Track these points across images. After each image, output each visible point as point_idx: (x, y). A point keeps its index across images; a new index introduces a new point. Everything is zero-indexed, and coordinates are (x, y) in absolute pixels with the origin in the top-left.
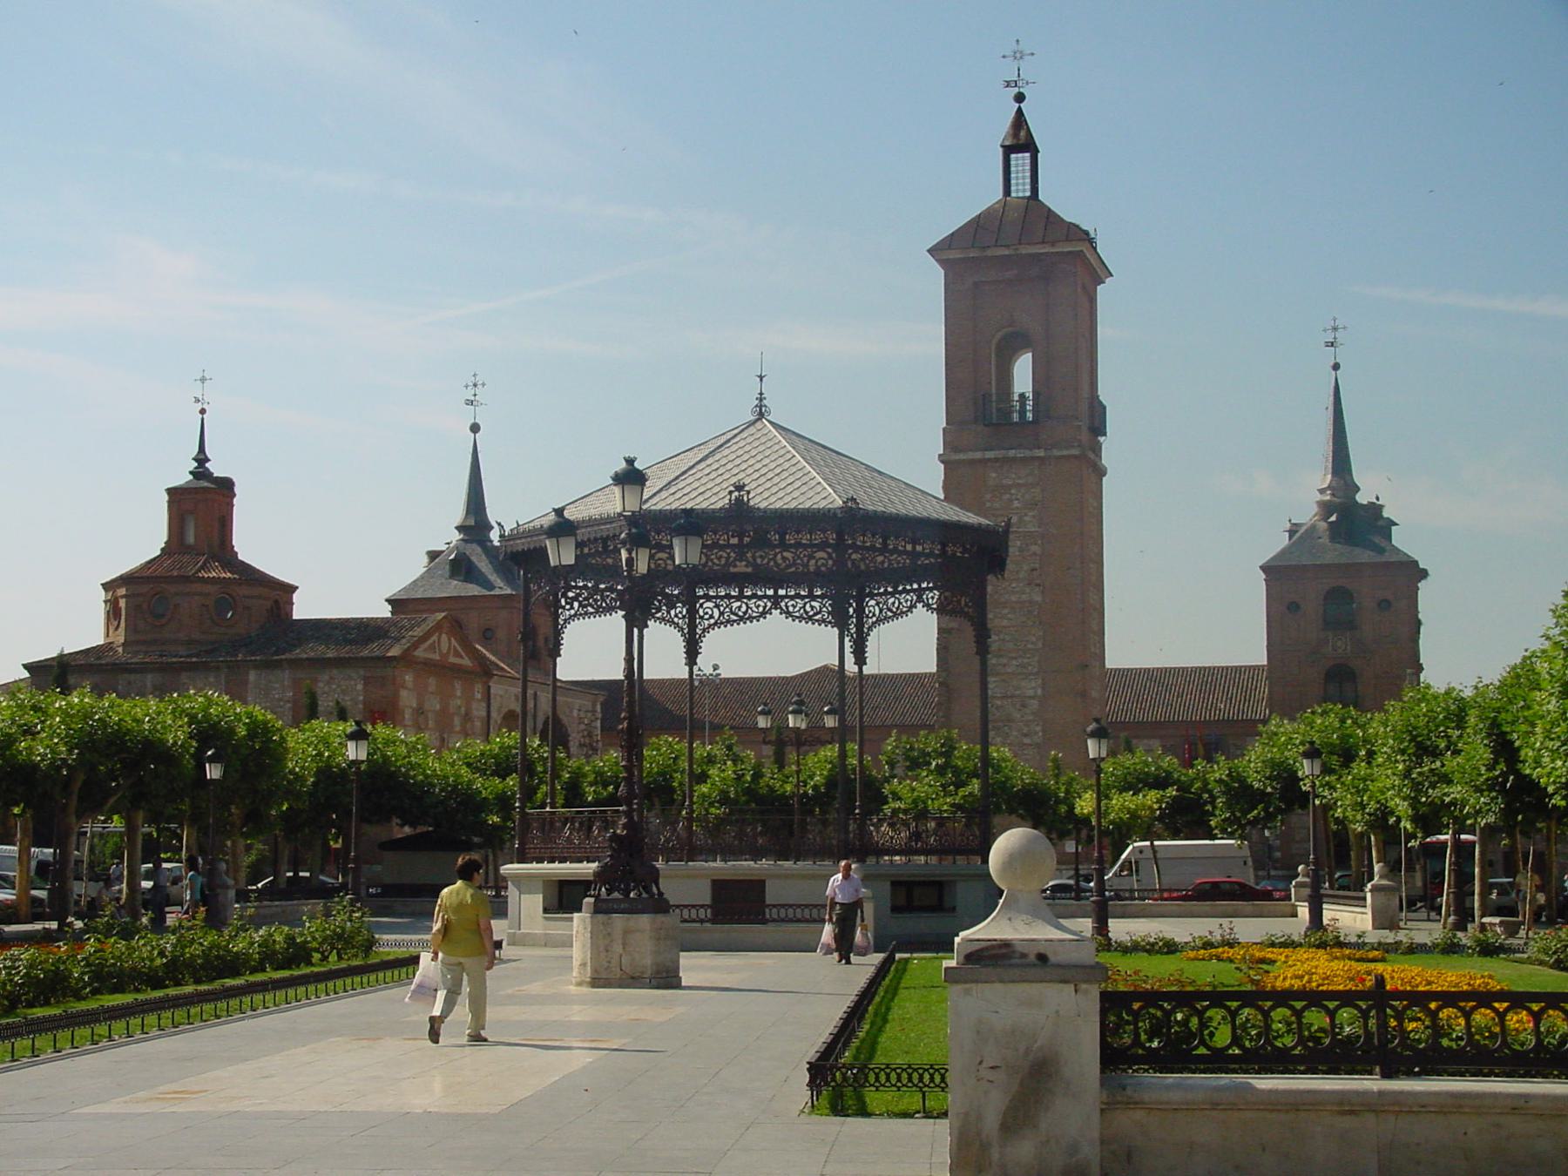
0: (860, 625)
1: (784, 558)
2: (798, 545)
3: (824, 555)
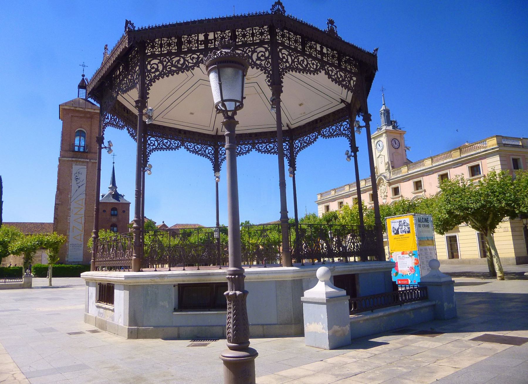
0: (292, 153)
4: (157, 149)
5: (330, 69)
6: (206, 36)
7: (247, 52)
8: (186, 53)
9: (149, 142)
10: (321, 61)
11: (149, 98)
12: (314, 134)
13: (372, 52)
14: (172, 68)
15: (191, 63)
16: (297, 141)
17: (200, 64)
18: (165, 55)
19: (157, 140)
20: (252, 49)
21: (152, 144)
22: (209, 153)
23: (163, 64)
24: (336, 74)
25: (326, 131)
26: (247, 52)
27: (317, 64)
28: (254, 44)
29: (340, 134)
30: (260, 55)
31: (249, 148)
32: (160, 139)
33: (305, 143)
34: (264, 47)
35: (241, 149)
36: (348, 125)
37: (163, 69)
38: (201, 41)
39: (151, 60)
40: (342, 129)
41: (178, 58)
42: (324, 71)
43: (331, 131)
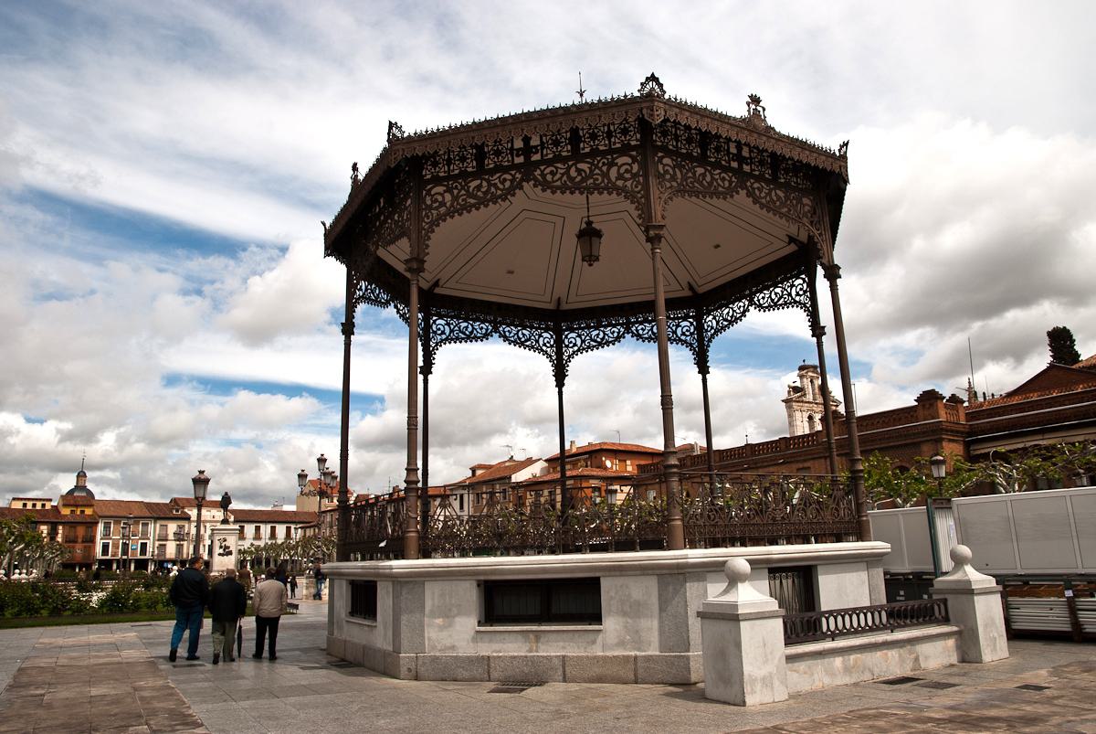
1: (579, 171)
2: (595, 153)
3: (627, 160)
4: (448, 340)
5: (756, 185)
6: (526, 140)
7: (600, 165)
8: (492, 172)
9: (434, 327)
10: (738, 172)
11: (428, 254)
12: (741, 304)
13: (835, 148)
14: (469, 200)
15: (500, 189)
16: (711, 317)
17: (517, 191)
18: (455, 178)
19: (448, 324)
20: (608, 159)
21: (439, 332)
22: (545, 345)
23: (452, 194)
24: (769, 194)
25: (763, 298)
26: (600, 165)
27: (731, 178)
28: (611, 151)
29: (790, 303)
30: (622, 170)
31: (619, 333)
32: (454, 322)
33: (726, 320)
34: (631, 156)
35: (605, 334)
36: (805, 285)
37: (453, 201)
38: (518, 150)
39: (432, 188)
40: (794, 293)
41: (478, 182)
42: (745, 191)
43: (773, 296)
